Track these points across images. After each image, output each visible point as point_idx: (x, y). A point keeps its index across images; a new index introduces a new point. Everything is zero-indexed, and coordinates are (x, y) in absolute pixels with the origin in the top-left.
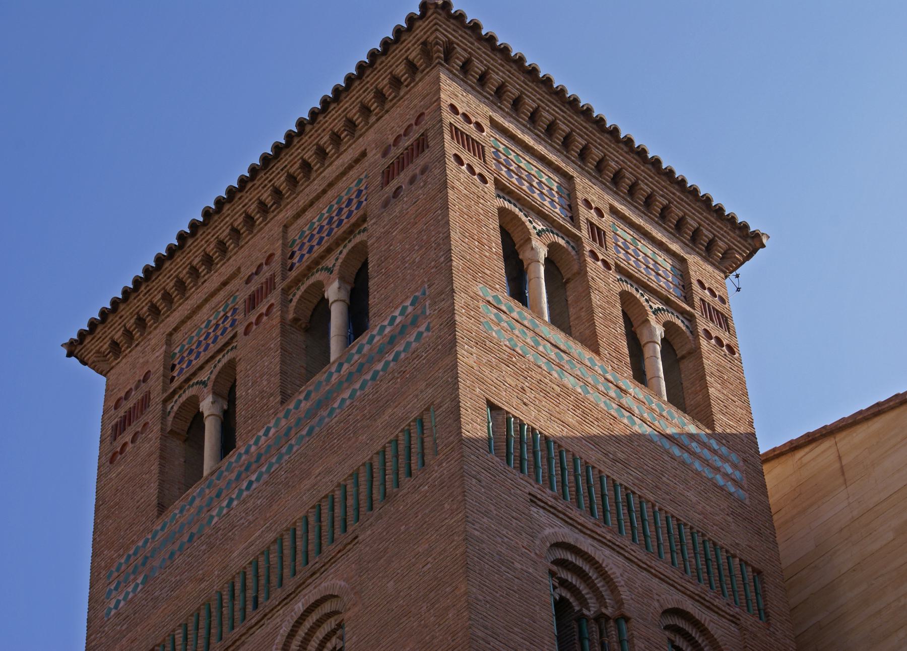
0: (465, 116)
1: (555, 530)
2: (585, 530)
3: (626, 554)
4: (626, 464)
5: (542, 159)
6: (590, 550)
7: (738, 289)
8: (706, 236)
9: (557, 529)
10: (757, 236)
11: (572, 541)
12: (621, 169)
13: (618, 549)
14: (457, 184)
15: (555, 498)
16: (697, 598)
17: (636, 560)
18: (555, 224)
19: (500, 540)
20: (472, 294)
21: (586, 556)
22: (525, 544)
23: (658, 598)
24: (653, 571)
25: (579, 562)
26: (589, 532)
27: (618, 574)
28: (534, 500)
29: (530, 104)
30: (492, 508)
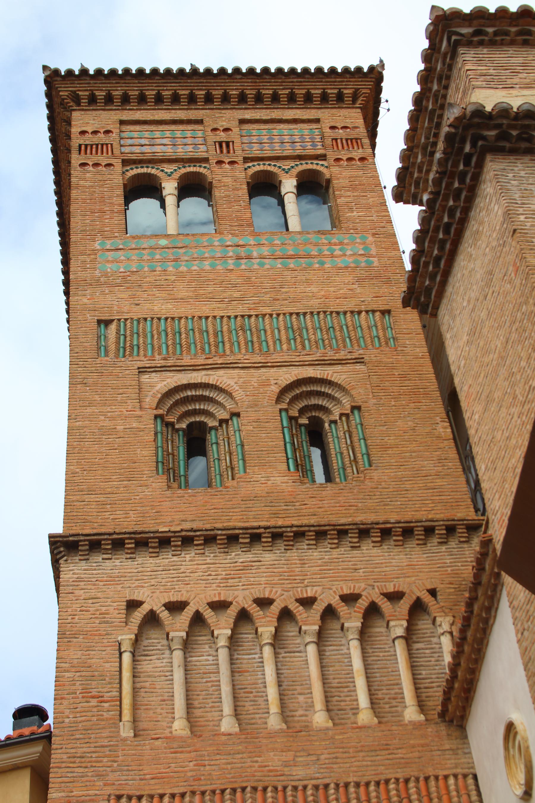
0: (95, 132)
1: (163, 383)
2: (197, 368)
3: (240, 365)
4: (240, 299)
5: (174, 122)
6: (205, 380)
7: (388, 110)
8: (332, 94)
9: (169, 380)
10: (372, 68)
11: (185, 382)
12: (243, 91)
13: (231, 366)
14: (82, 183)
15: (165, 359)
16: (317, 363)
17: (250, 365)
18: (185, 160)
19: (102, 418)
20: (89, 252)
21: (203, 385)
22: (130, 408)
23: (276, 381)
24: (269, 364)
25: (199, 392)
26: (200, 367)
27: (232, 383)
28: (142, 371)
29: (151, 94)
30: (97, 397)
